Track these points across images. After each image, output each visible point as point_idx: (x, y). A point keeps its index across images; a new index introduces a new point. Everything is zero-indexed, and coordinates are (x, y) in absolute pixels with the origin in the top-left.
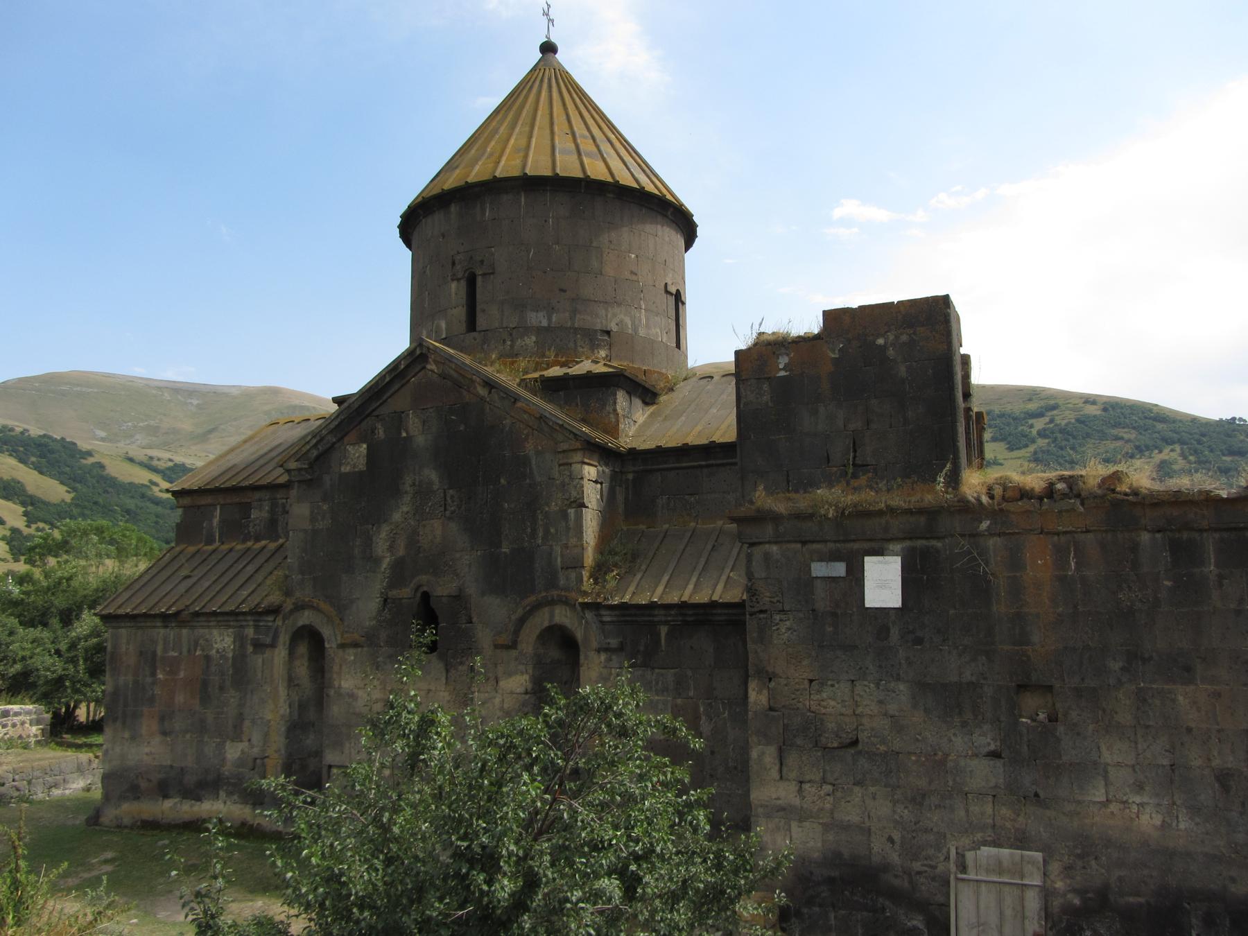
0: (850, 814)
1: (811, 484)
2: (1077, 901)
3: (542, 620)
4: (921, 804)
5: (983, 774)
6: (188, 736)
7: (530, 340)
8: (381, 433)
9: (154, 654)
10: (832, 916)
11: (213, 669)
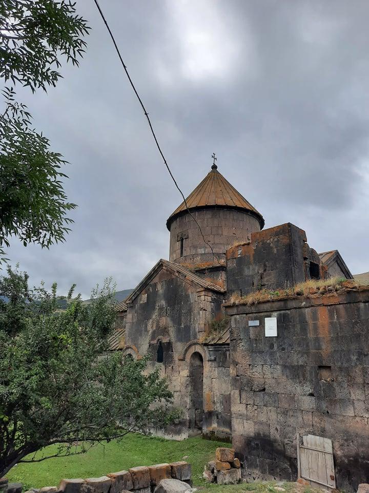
0: (263, 418)
1: (247, 293)
2: (346, 461)
4: (286, 415)
5: (308, 403)
7: (199, 258)
10: (258, 460)
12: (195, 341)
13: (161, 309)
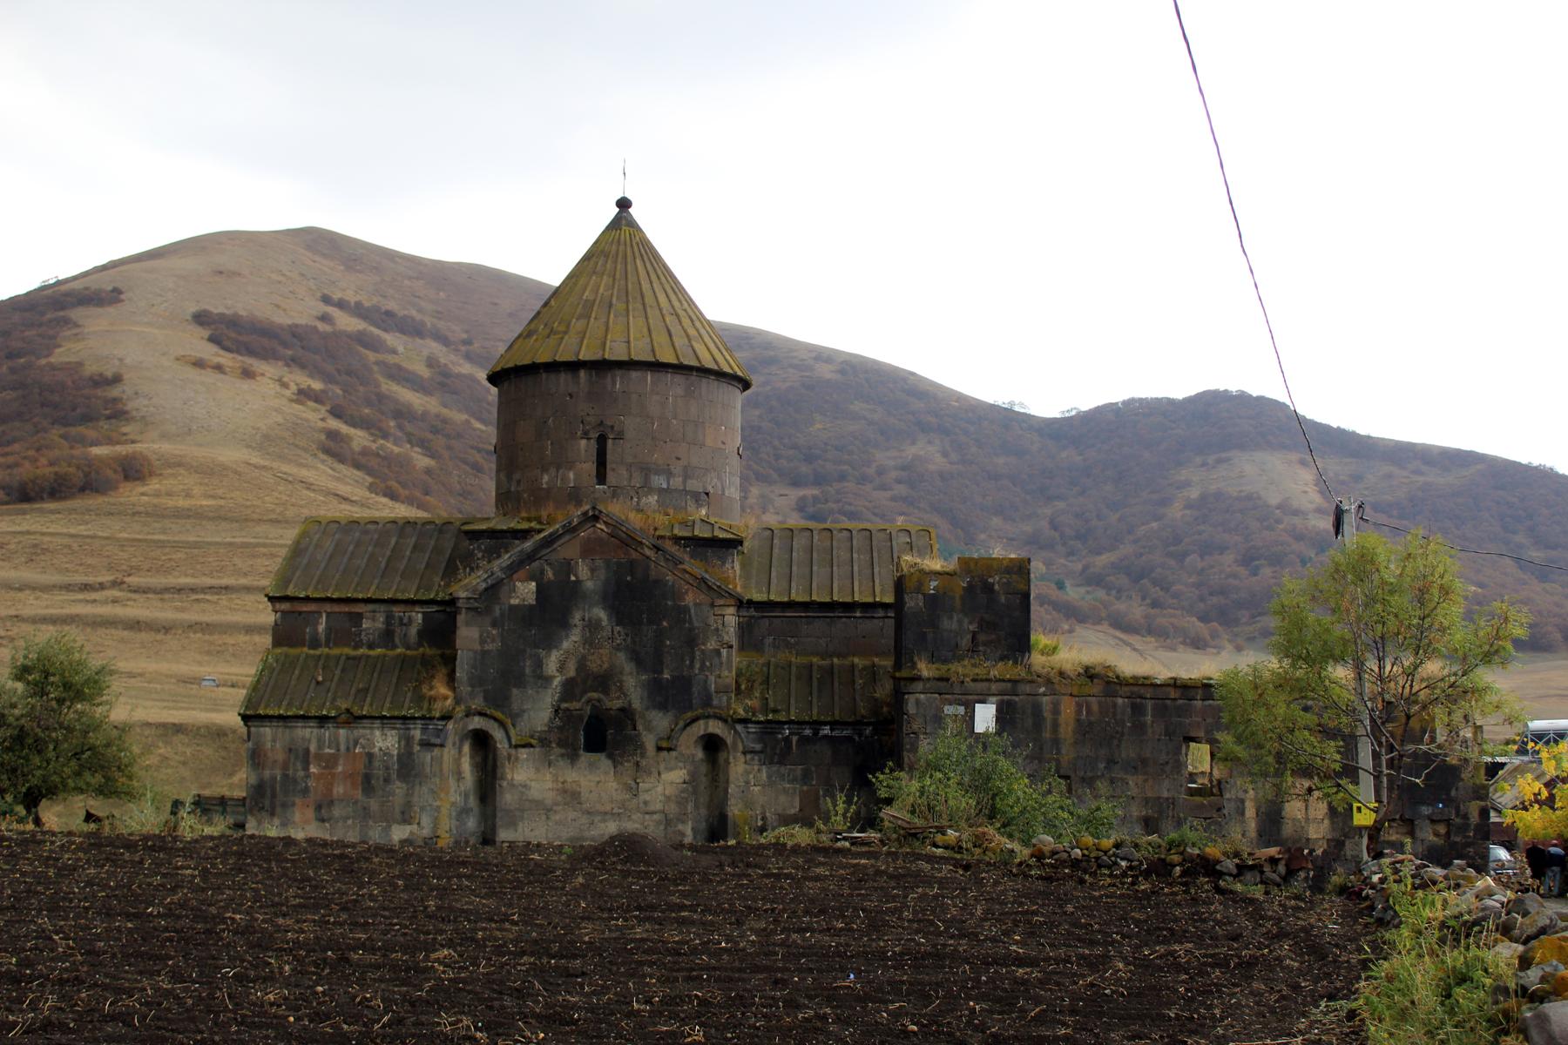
3: (700, 728)
6: (350, 822)
8: (550, 574)
9: (307, 751)
11: (376, 764)
12: (711, 711)
13: (592, 626)
